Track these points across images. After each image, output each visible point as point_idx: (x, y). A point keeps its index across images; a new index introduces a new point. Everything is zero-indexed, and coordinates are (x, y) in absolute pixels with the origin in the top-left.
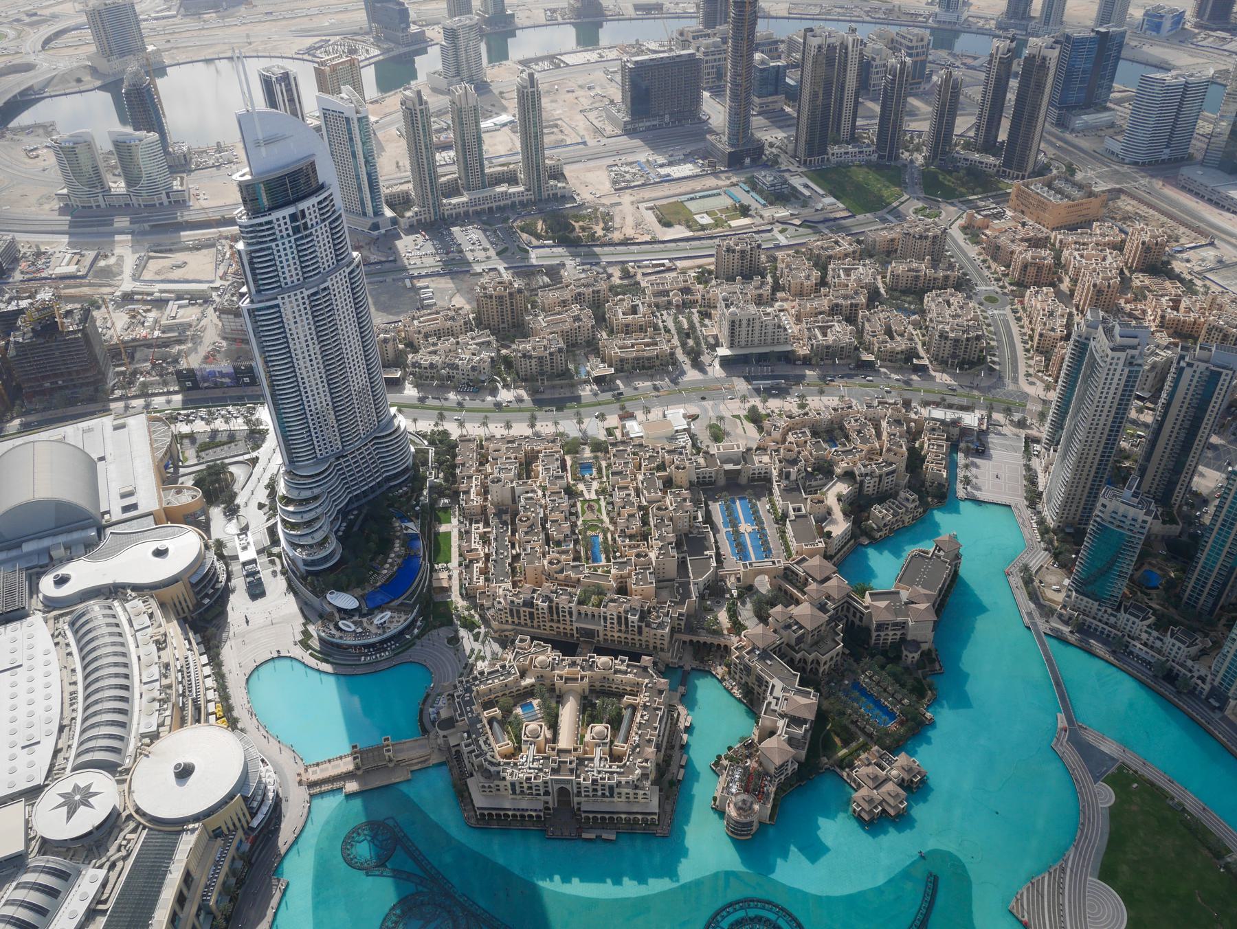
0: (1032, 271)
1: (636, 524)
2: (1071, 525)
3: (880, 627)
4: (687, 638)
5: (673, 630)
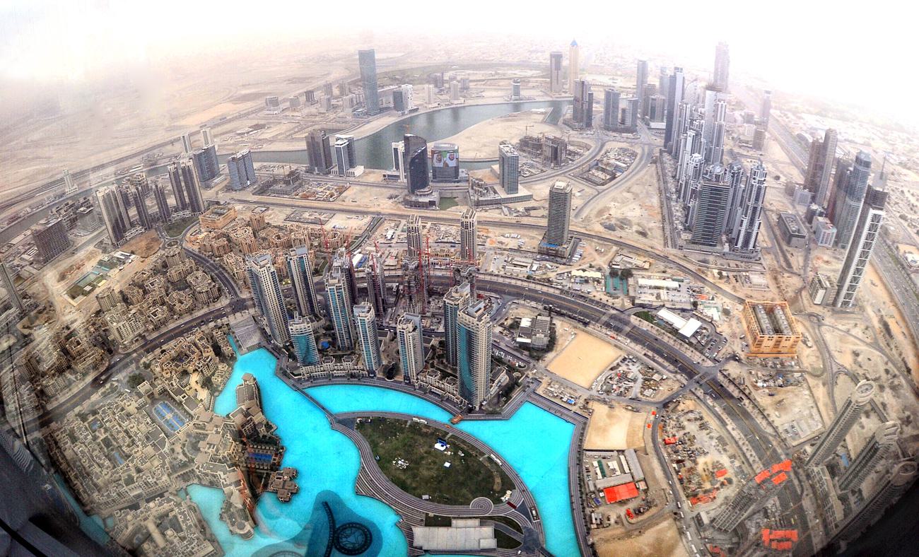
0: (221, 249)
1: (127, 439)
2: (287, 341)
3: (243, 426)
4: (176, 475)
5: (169, 475)
